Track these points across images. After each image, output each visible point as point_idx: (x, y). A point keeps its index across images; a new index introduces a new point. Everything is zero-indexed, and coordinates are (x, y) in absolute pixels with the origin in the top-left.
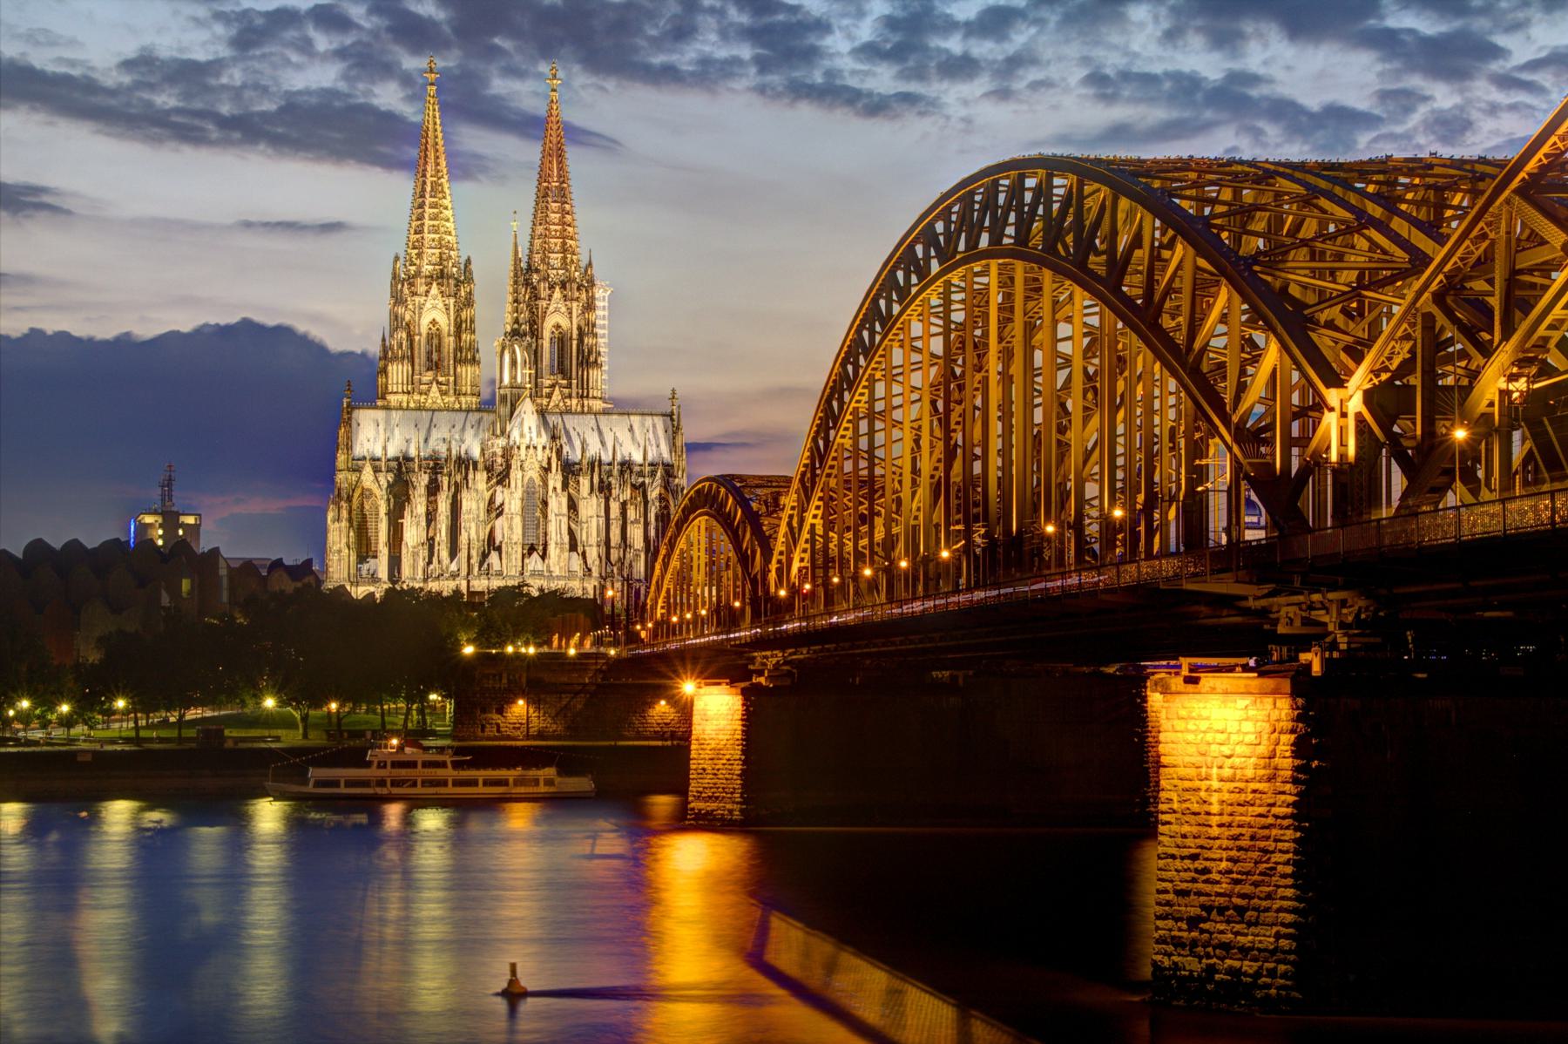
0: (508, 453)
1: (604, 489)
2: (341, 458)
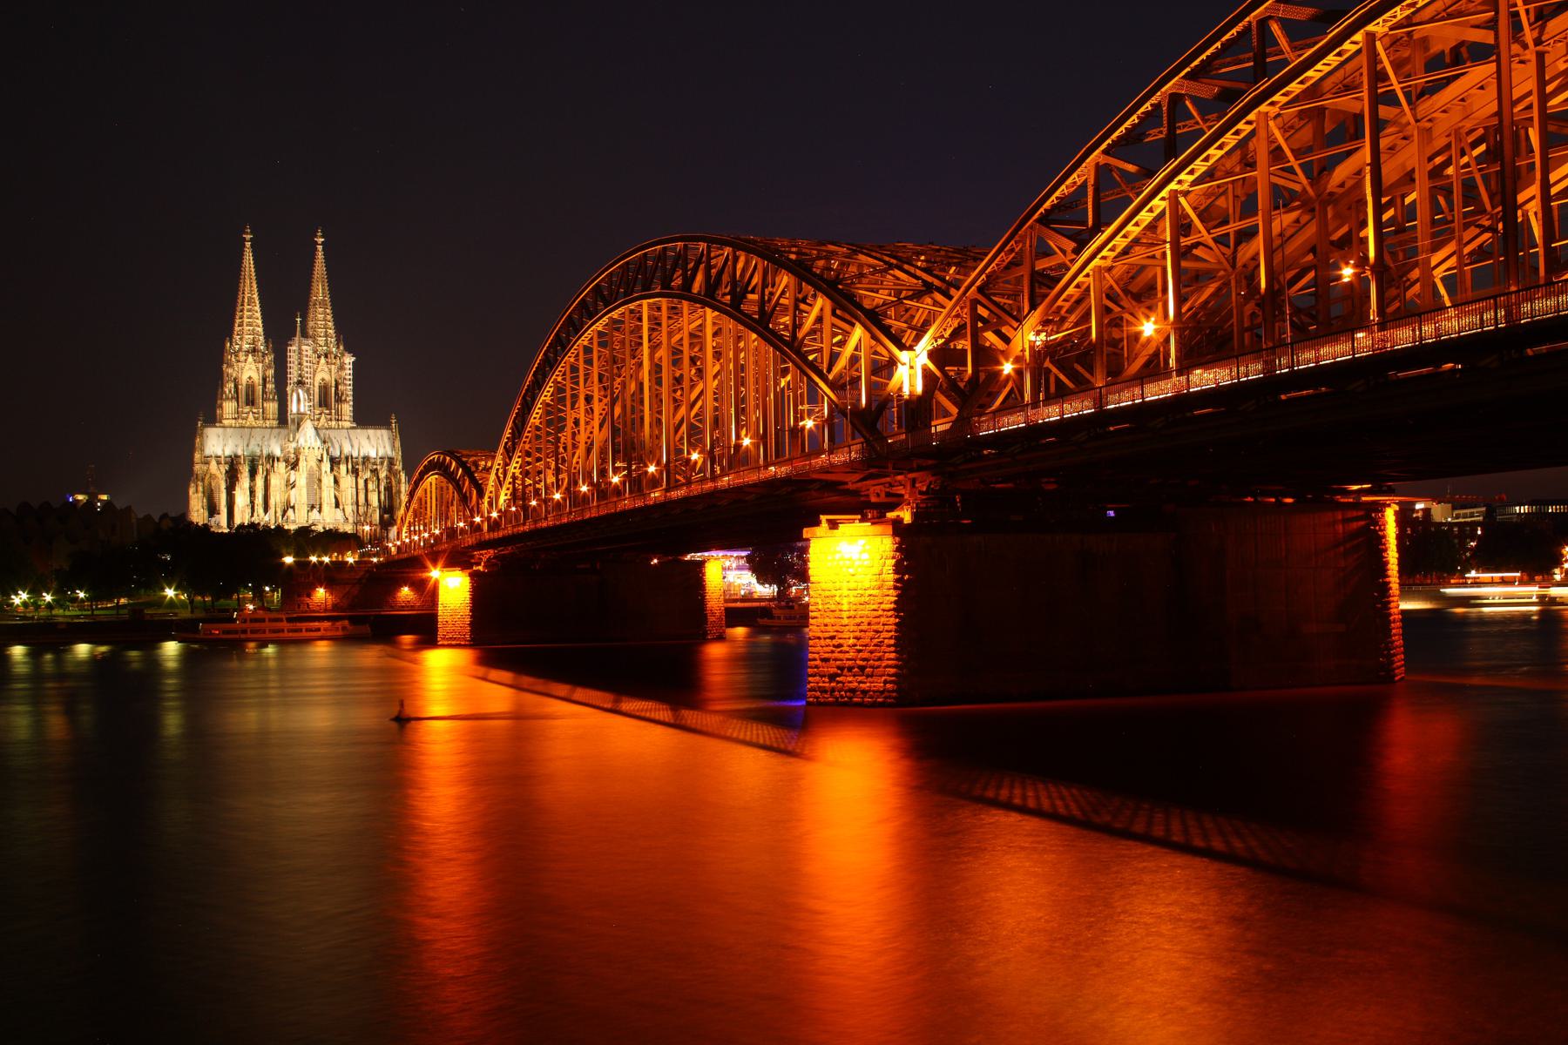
0: (297, 452)
1: (355, 472)
2: (197, 456)
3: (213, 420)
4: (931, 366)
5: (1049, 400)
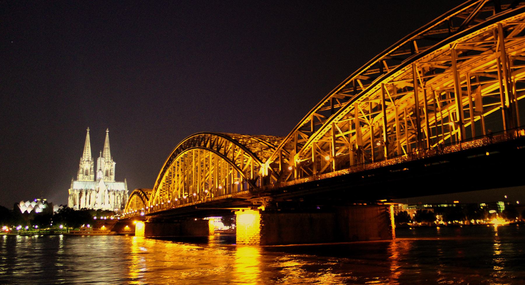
1: (114, 194)
3: (76, 179)
4: (270, 168)
5: (301, 178)
